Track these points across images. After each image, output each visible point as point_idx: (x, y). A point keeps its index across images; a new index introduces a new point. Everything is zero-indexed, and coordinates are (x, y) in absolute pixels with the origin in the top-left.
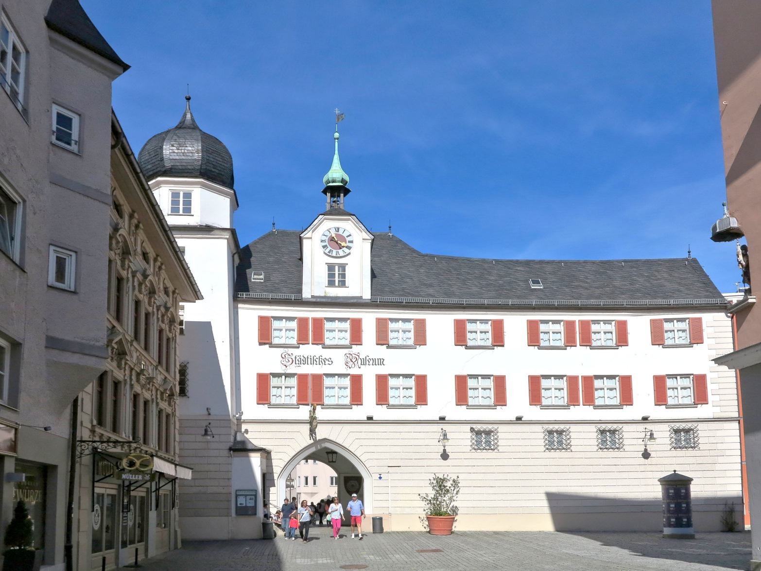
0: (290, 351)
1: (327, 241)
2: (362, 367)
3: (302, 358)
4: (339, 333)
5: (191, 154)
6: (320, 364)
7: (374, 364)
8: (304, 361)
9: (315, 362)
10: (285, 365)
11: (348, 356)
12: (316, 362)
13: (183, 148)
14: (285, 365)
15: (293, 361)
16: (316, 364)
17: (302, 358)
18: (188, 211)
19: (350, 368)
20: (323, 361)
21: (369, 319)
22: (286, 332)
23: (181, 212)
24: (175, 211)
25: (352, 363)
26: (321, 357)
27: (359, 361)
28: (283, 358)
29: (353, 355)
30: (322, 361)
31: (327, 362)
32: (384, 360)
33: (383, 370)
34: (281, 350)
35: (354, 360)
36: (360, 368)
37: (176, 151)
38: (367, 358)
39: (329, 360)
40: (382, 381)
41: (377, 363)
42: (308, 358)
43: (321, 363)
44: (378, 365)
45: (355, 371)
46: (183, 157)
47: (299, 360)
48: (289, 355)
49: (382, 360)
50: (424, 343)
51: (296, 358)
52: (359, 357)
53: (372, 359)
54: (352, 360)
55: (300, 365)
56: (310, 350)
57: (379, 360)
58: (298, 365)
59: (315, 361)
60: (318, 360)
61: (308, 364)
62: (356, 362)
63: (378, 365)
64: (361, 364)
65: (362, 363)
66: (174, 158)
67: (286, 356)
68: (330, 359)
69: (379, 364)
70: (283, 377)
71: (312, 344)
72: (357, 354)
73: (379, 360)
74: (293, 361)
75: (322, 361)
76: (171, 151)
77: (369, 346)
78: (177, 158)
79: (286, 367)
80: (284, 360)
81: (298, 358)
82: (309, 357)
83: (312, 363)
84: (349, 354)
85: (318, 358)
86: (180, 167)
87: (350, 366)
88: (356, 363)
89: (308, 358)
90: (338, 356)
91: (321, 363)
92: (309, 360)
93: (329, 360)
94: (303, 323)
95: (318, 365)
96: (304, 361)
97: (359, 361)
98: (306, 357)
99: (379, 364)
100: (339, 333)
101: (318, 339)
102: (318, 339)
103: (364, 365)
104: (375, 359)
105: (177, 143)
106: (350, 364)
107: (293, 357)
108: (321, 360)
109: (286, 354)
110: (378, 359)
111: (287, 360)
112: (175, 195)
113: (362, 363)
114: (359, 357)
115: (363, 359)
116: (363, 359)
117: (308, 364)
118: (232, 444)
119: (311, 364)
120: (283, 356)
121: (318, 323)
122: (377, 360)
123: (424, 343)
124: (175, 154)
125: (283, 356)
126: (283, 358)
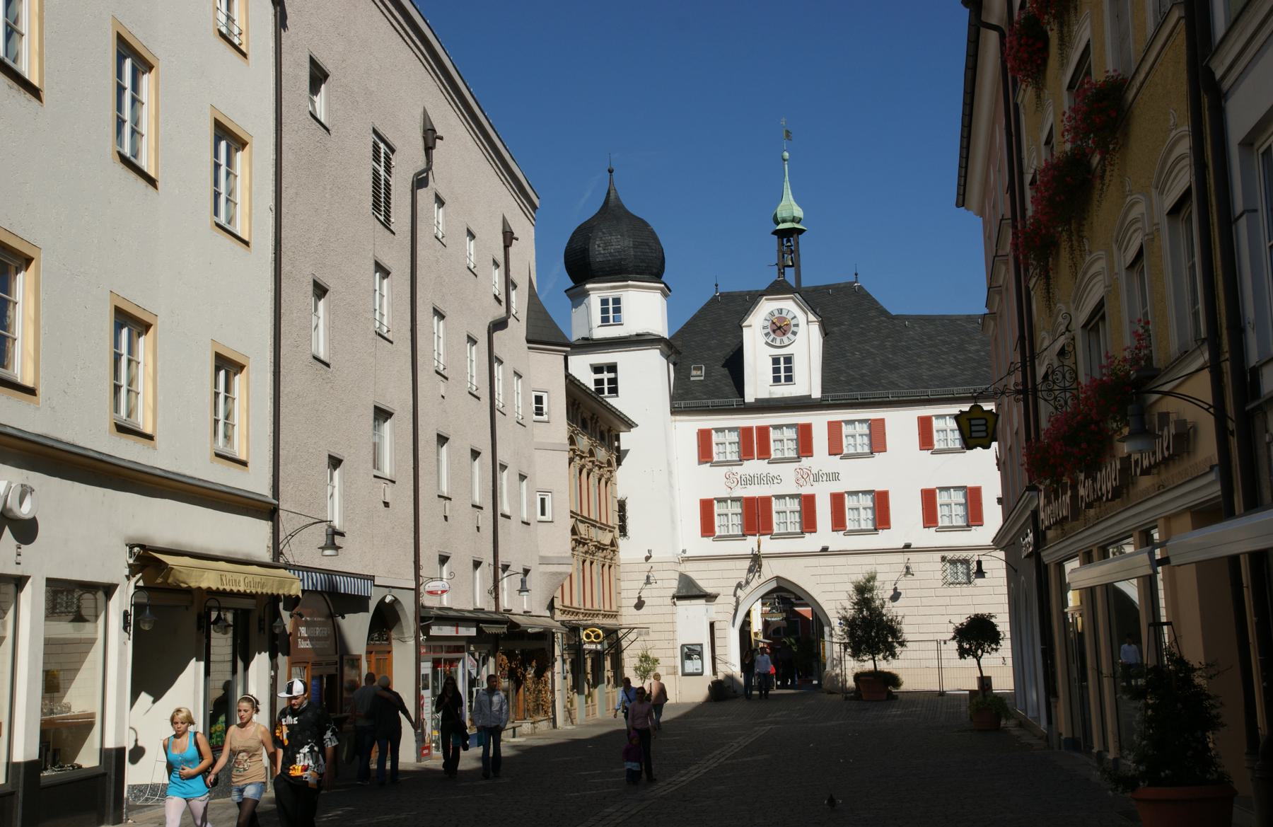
0: (735, 469)
3: (748, 477)
4: (782, 443)
5: (617, 254)
8: (749, 480)
11: (798, 470)
13: (609, 247)
17: (748, 477)
18: (617, 321)
21: (819, 422)
22: (726, 446)
23: (611, 322)
24: (605, 320)
30: (771, 480)
33: (838, 488)
34: (725, 469)
35: (805, 477)
37: (602, 252)
38: (820, 473)
40: (838, 501)
41: (831, 479)
43: (769, 482)
45: (806, 491)
46: (610, 258)
49: (837, 474)
50: (883, 448)
51: (741, 477)
54: (803, 476)
56: (754, 466)
60: (765, 479)
62: (808, 478)
66: (601, 260)
70: (729, 501)
71: (758, 459)
75: (771, 480)
76: (597, 253)
77: (821, 458)
78: (604, 259)
81: (743, 477)
82: (756, 475)
86: (608, 269)
90: (787, 470)
91: (769, 482)
92: (756, 478)
94: (745, 433)
95: (766, 485)
96: (749, 480)
100: (782, 443)
101: (764, 453)
102: (764, 453)
105: (603, 242)
112: (604, 302)
118: (675, 590)
121: (763, 432)
122: (831, 475)
123: (883, 448)
124: (602, 256)
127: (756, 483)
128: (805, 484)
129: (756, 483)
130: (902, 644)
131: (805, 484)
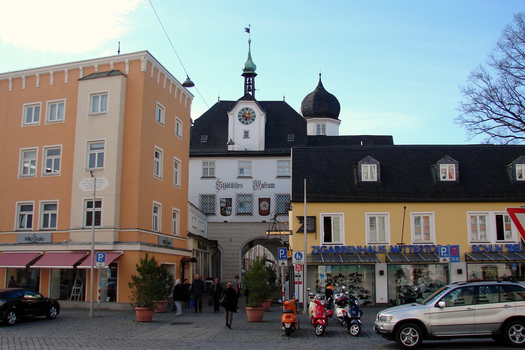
1: (241, 116)
7: (269, 187)
9: (233, 186)
10: (218, 189)
14: (218, 189)
15: (222, 186)
19: (256, 190)
20: (238, 186)
28: (217, 185)
31: (240, 187)
32: (274, 184)
36: (261, 190)
39: (241, 185)
41: (270, 187)
42: (230, 184)
43: (236, 187)
44: (271, 188)
47: (225, 185)
48: (220, 182)
49: (273, 185)
51: (223, 184)
55: (226, 188)
58: (224, 188)
59: (233, 186)
60: (235, 185)
61: (230, 188)
64: (262, 187)
68: (242, 184)
69: (272, 187)
72: (259, 181)
74: (222, 186)
79: (218, 189)
88: (259, 187)
89: (230, 184)
91: (236, 187)
92: (231, 185)
97: (261, 185)
98: (229, 184)
99: (272, 187)
104: (270, 184)
106: (256, 187)
108: (236, 185)
110: (271, 184)
116: (263, 184)
117: (230, 188)
119: (231, 188)
120: (217, 184)
122: (270, 185)
125: (217, 184)
126: (217, 185)
127: (231, 187)
128: (257, 189)
129: (231, 187)
130: (258, 258)
131: (257, 189)
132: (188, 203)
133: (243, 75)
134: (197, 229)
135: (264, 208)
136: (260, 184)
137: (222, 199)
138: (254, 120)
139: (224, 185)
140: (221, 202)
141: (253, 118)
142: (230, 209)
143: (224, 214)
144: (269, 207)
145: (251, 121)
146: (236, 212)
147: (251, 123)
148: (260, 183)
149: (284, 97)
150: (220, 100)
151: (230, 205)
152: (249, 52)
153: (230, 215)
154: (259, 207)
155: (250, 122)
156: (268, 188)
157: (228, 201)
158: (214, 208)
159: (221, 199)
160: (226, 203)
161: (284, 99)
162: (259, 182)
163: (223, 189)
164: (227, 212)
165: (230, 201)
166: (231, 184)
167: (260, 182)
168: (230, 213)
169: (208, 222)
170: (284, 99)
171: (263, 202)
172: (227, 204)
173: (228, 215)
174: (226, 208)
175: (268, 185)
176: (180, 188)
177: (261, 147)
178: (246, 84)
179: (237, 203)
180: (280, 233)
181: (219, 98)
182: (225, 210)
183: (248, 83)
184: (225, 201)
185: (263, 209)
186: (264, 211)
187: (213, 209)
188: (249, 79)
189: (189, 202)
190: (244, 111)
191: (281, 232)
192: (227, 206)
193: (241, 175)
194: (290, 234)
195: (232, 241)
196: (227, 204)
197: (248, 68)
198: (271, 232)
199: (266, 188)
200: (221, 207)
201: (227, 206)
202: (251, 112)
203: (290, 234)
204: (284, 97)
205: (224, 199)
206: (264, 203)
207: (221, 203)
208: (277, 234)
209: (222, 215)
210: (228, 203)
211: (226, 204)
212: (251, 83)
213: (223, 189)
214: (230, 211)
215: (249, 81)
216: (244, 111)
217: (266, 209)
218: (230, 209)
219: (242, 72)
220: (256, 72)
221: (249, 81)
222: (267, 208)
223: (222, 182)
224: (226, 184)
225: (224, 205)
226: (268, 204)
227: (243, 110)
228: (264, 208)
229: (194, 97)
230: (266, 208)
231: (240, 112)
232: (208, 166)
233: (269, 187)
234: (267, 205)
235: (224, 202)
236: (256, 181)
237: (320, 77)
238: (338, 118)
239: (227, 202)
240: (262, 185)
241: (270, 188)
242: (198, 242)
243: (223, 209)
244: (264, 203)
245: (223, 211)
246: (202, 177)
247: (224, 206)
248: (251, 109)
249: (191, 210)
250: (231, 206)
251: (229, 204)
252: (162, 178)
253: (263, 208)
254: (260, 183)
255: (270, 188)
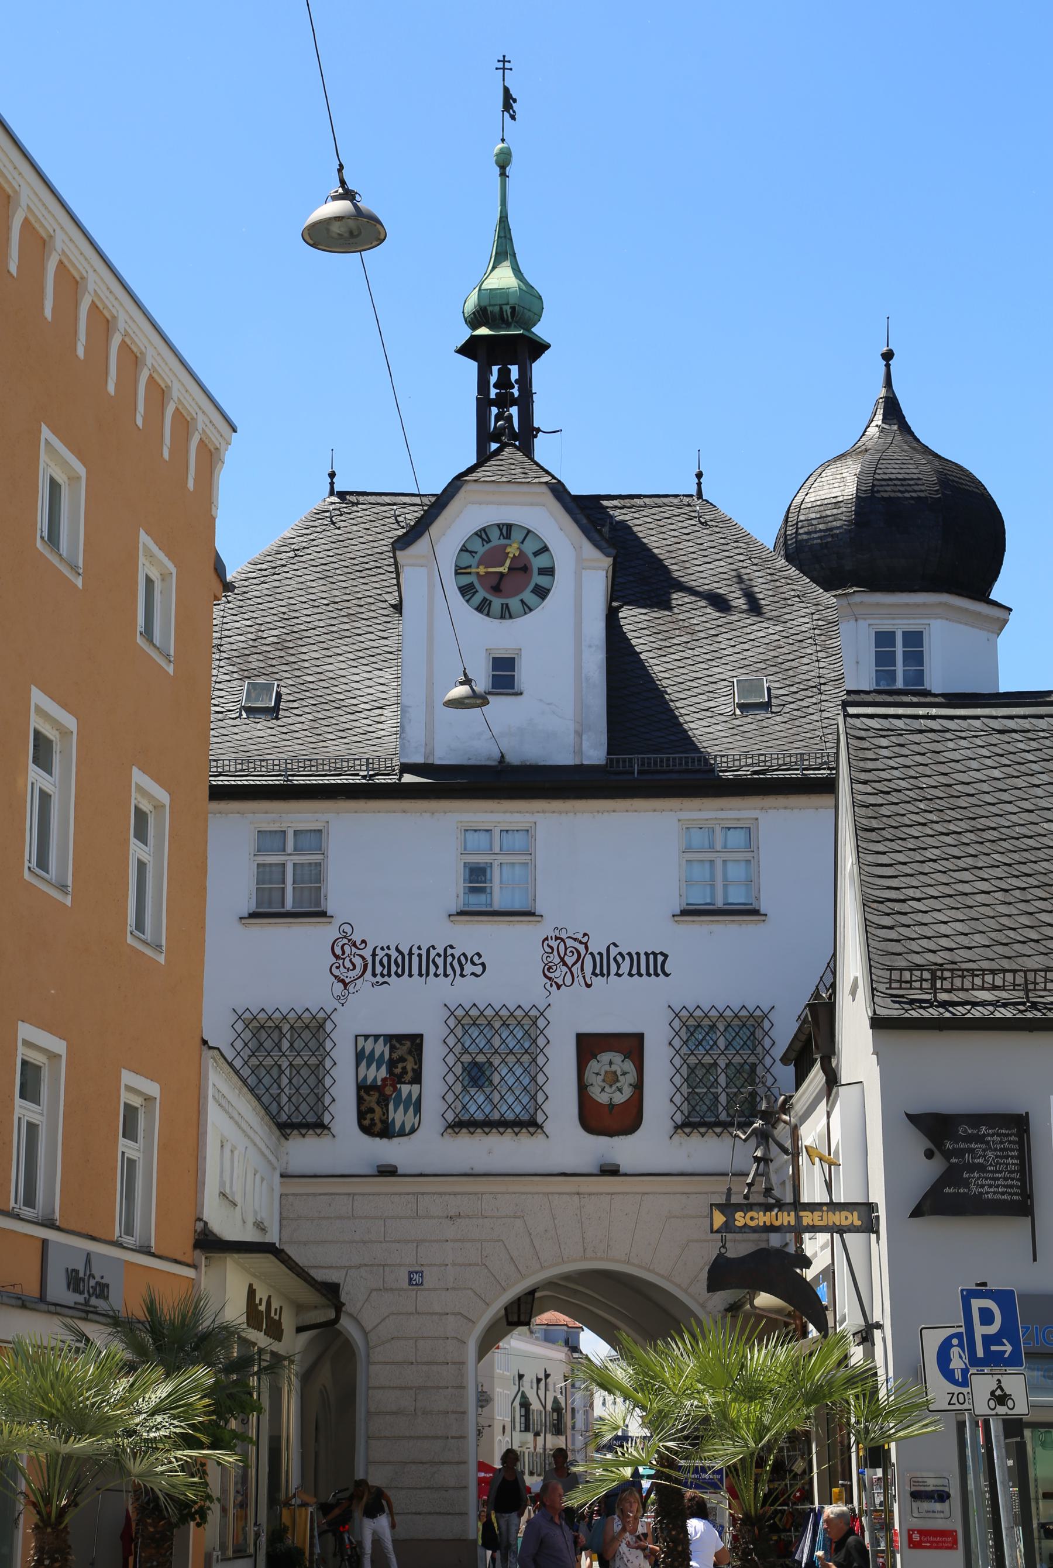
2: (598, 981)
3: (394, 954)
6: (446, 975)
7: (634, 971)
10: (343, 981)
11: (554, 944)
12: (437, 967)
14: (343, 981)
15: (366, 967)
16: (436, 975)
17: (394, 954)
19: (559, 987)
20: (456, 964)
25: (565, 969)
26: (449, 951)
27: (588, 962)
28: (337, 957)
29: (570, 943)
31: (469, 968)
32: (666, 956)
35: (570, 961)
36: (588, 986)
38: (614, 952)
39: (476, 959)
41: (643, 970)
42: (410, 954)
43: (449, 971)
47: (385, 961)
48: (354, 945)
49: (660, 958)
51: (374, 955)
52: (587, 948)
53: (629, 954)
55: (386, 979)
57: (651, 957)
58: (379, 979)
60: (440, 961)
61: (410, 975)
63: (649, 974)
64: (594, 974)
65: (598, 971)
67: (346, 948)
68: (479, 955)
69: (652, 971)
72: (579, 936)
73: (651, 957)
74: (366, 967)
79: (345, 985)
80: (341, 962)
81: (380, 954)
82: (415, 951)
83: (424, 971)
84: (557, 938)
85: (442, 954)
87: (560, 982)
89: (410, 954)
91: (449, 971)
92: (415, 959)
93: (476, 958)
97: (589, 958)
98: (406, 952)
99: (652, 971)
103: (603, 975)
104: (638, 954)
107: (367, 953)
108: (449, 959)
109: (345, 941)
110: (646, 954)
111: (348, 964)
113: (598, 971)
114: (587, 948)
115: (600, 954)
116: (600, 954)
117: (410, 975)
119: (420, 975)
120: (338, 951)
122: (643, 958)
125: (338, 951)
132: (205, 1048)
133: (468, 349)
134: (238, 1209)
135: (607, 1089)
136: (583, 951)
137: (366, 1037)
138: (549, 591)
139: (378, 959)
140: (359, 1056)
141: (543, 581)
142: (414, 1098)
143: (379, 1126)
144: (638, 1087)
145: (528, 596)
146: (450, 1116)
147: (527, 609)
148: (582, 948)
149: (699, 475)
150: (337, 489)
151: (410, 1074)
152: (504, 220)
153: (413, 1130)
154: (583, 1088)
155: (522, 601)
156: (630, 975)
157: (402, 1050)
158: (319, 1091)
159: (361, 1040)
160: (392, 1064)
161: (699, 484)
162: (575, 940)
163: (374, 980)
164: (398, 1116)
165: (410, 1052)
166: (420, 956)
167: (584, 940)
168: (410, 1120)
169: (282, 1176)
170: (699, 484)
171: (605, 1057)
172: (398, 1071)
173: (402, 1133)
174: (388, 1090)
175: (627, 958)
176: (162, 959)
177: (585, 745)
178: (483, 404)
179: (451, 1059)
180: (798, 1219)
181: (332, 475)
182: (383, 1102)
183: (493, 393)
184: (381, 1048)
185: (603, 1098)
186: (611, 1106)
187: (311, 1099)
188: (504, 374)
189: (205, 1042)
190: (489, 541)
191: (802, 1214)
192: (396, 1078)
193: (477, 902)
194: (858, 1223)
195: (426, 1285)
196: (398, 1071)
197: (497, 309)
198: (739, 1215)
199: (618, 975)
200: (363, 1089)
201: (396, 1078)
202: (530, 547)
203: (858, 1223)
204: (699, 475)
205: (377, 1037)
206: (611, 1063)
207: (364, 1063)
208: (777, 1224)
209: (367, 1130)
210: (402, 1059)
211: (390, 1071)
212: (516, 393)
213: (374, 980)
214: (411, 1109)
215: (504, 382)
216: (489, 541)
217: (619, 1099)
218: (410, 1093)
219: (464, 333)
220: (541, 331)
221: (504, 382)
222: (628, 1092)
223: (363, 942)
224: (389, 956)
225: (377, 1074)
226: (629, 1066)
227: (482, 534)
228: (607, 1089)
229: (235, 431)
230: (620, 1090)
231: (464, 549)
232: (284, 850)
233: (634, 971)
234: (624, 1074)
235: (377, 1055)
236: (564, 935)
237: (888, 366)
238: (994, 596)
239: (395, 1056)
240: (598, 958)
241: (640, 975)
242: (251, 1286)
243: (372, 1100)
244: (611, 1063)
245: (372, 1111)
246: (253, 915)
247: (379, 1083)
248: (529, 531)
249: (218, 1097)
250: (417, 1079)
251: (409, 1068)
252: (70, 889)
253: (603, 1090)
254: (582, 948)
255: (640, 975)
